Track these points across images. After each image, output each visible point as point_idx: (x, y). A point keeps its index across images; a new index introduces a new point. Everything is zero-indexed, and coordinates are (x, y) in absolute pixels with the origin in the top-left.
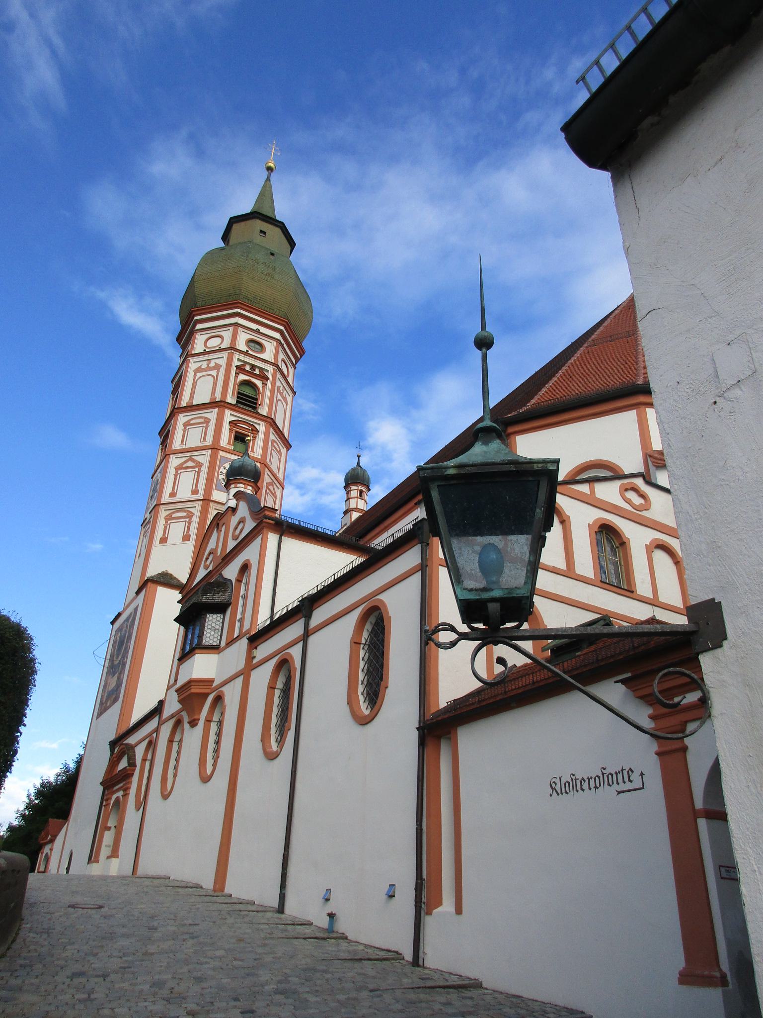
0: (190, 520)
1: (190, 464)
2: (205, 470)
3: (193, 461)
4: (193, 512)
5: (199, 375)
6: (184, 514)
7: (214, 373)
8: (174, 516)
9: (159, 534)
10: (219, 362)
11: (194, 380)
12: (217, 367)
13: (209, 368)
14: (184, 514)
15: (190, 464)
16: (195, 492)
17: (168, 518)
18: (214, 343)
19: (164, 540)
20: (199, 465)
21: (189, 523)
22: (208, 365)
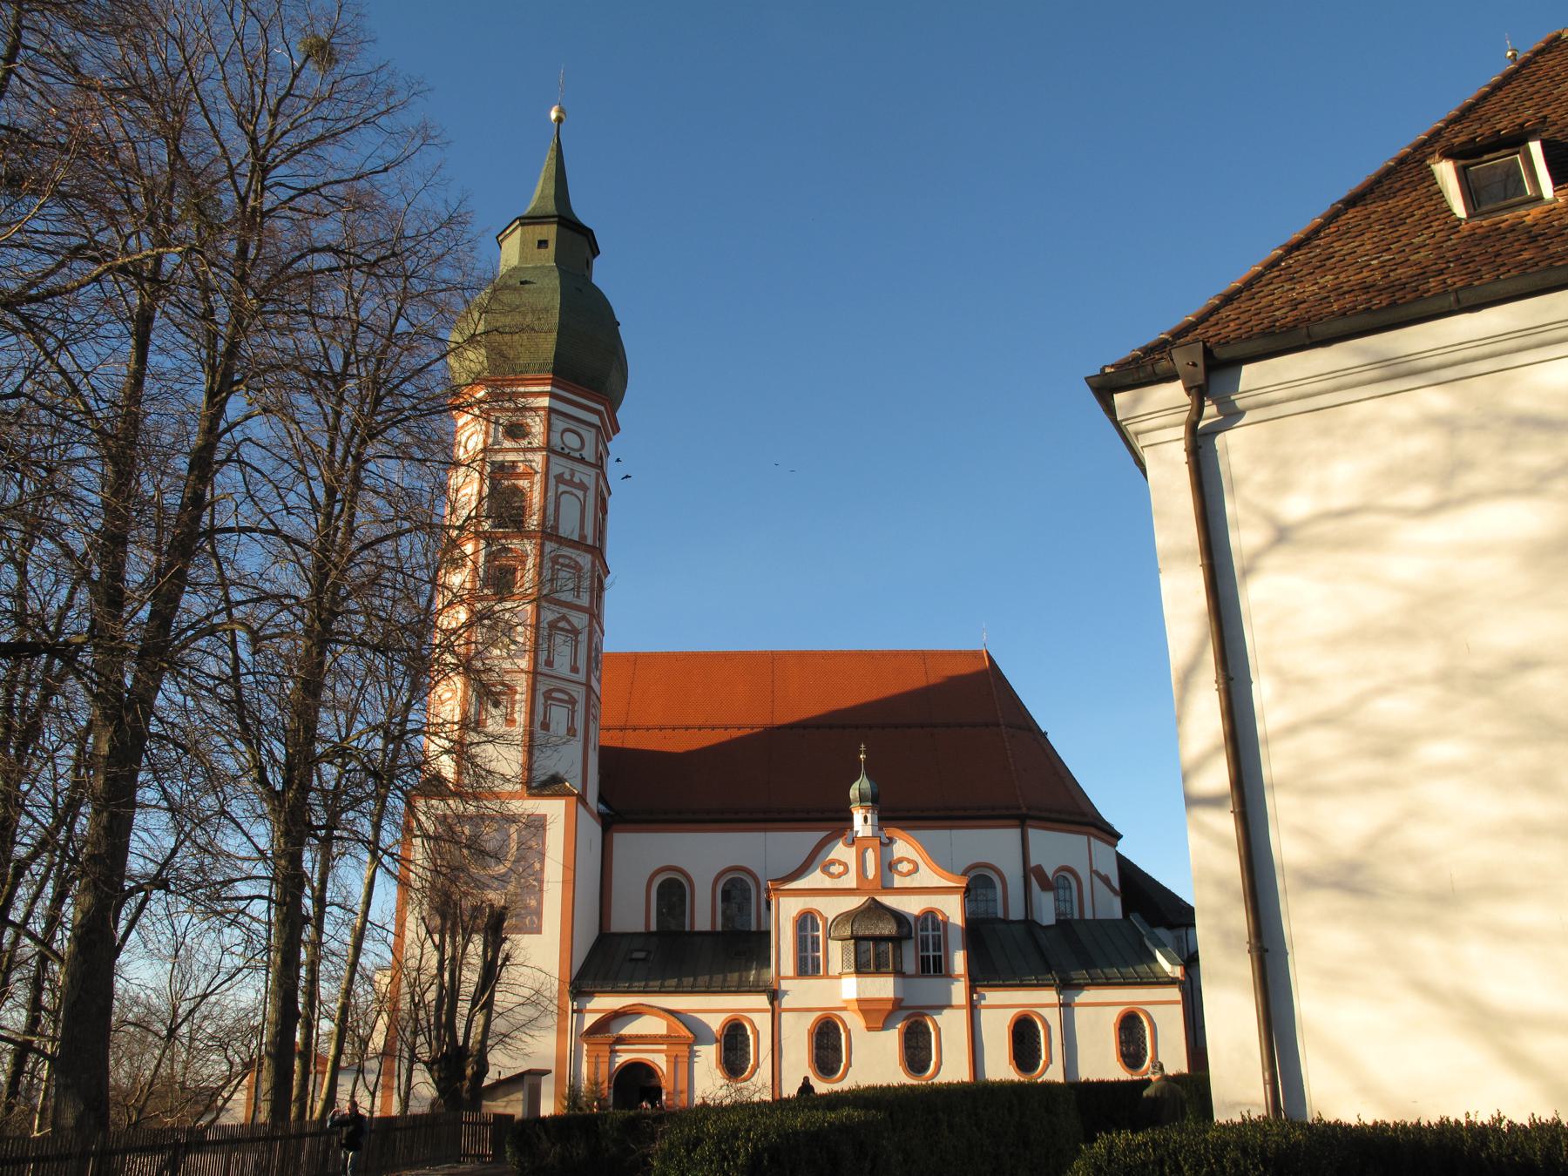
0: (573, 707)
1: (562, 624)
2: (583, 638)
3: (569, 622)
4: (575, 694)
5: (562, 488)
6: (566, 698)
7: (580, 494)
8: (555, 695)
9: (539, 718)
10: (586, 480)
11: (556, 493)
12: (582, 486)
13: (570, 483)
14: (566, 698)
15: (562, 624)
16: (575, 669)
17: (548, 695)
18: (572, 441)
19: (545, 726)
20: (575, 632)
21: (573, 712)
22: (572, 475)
